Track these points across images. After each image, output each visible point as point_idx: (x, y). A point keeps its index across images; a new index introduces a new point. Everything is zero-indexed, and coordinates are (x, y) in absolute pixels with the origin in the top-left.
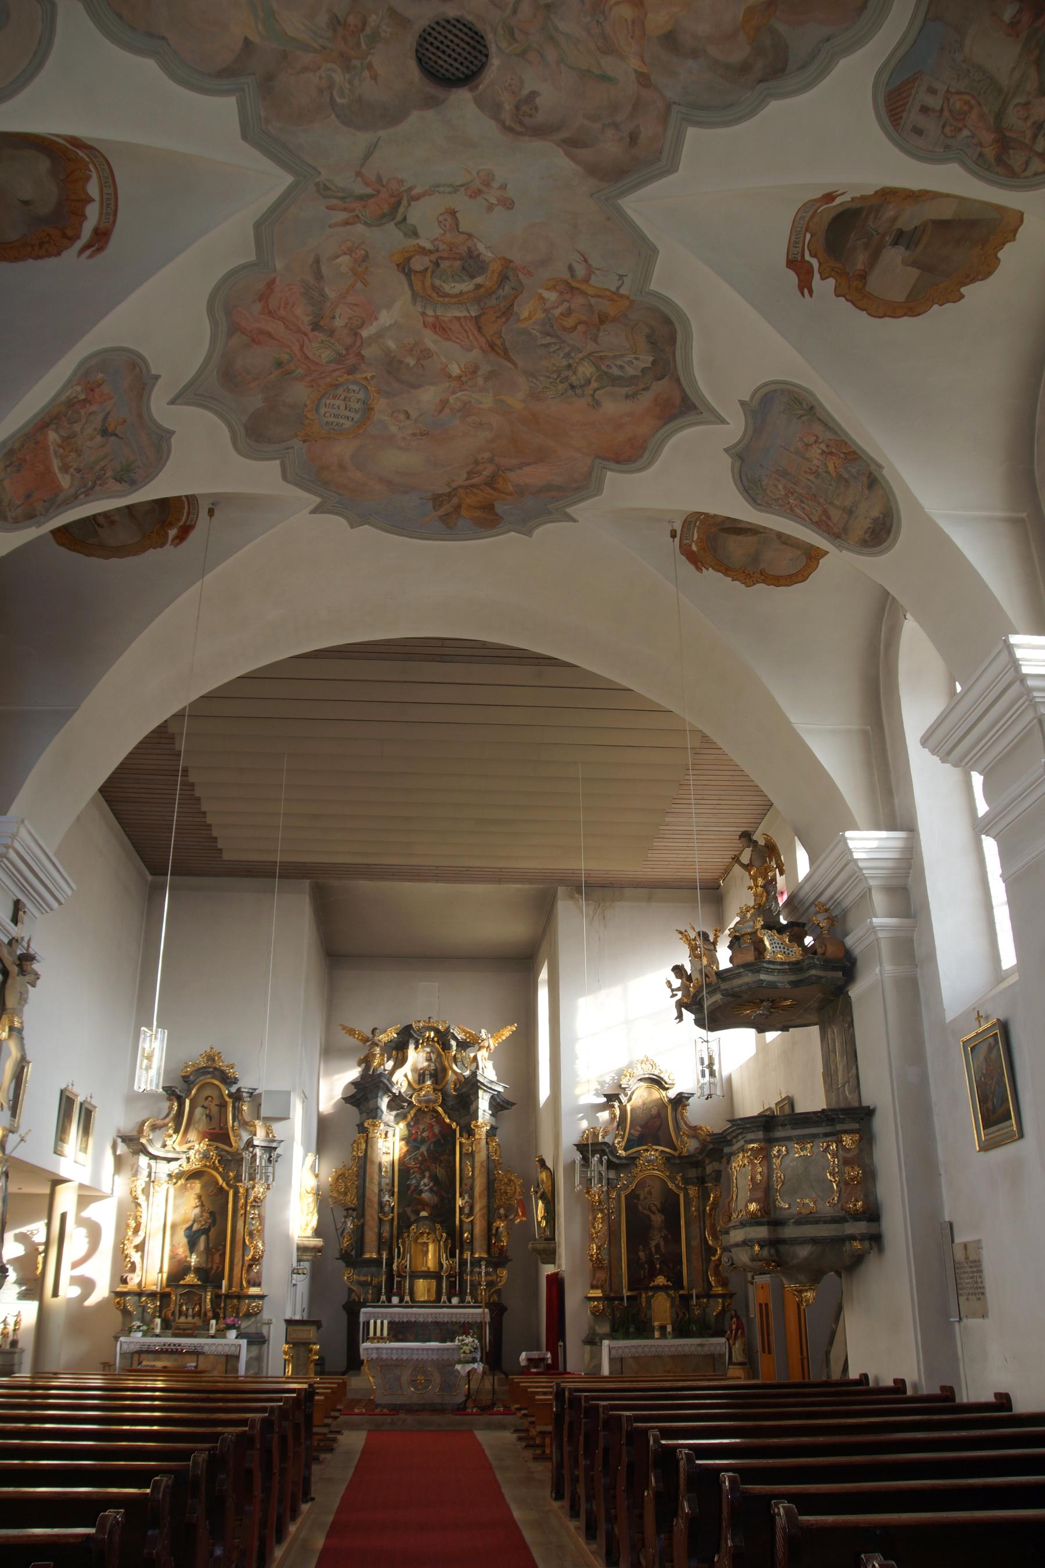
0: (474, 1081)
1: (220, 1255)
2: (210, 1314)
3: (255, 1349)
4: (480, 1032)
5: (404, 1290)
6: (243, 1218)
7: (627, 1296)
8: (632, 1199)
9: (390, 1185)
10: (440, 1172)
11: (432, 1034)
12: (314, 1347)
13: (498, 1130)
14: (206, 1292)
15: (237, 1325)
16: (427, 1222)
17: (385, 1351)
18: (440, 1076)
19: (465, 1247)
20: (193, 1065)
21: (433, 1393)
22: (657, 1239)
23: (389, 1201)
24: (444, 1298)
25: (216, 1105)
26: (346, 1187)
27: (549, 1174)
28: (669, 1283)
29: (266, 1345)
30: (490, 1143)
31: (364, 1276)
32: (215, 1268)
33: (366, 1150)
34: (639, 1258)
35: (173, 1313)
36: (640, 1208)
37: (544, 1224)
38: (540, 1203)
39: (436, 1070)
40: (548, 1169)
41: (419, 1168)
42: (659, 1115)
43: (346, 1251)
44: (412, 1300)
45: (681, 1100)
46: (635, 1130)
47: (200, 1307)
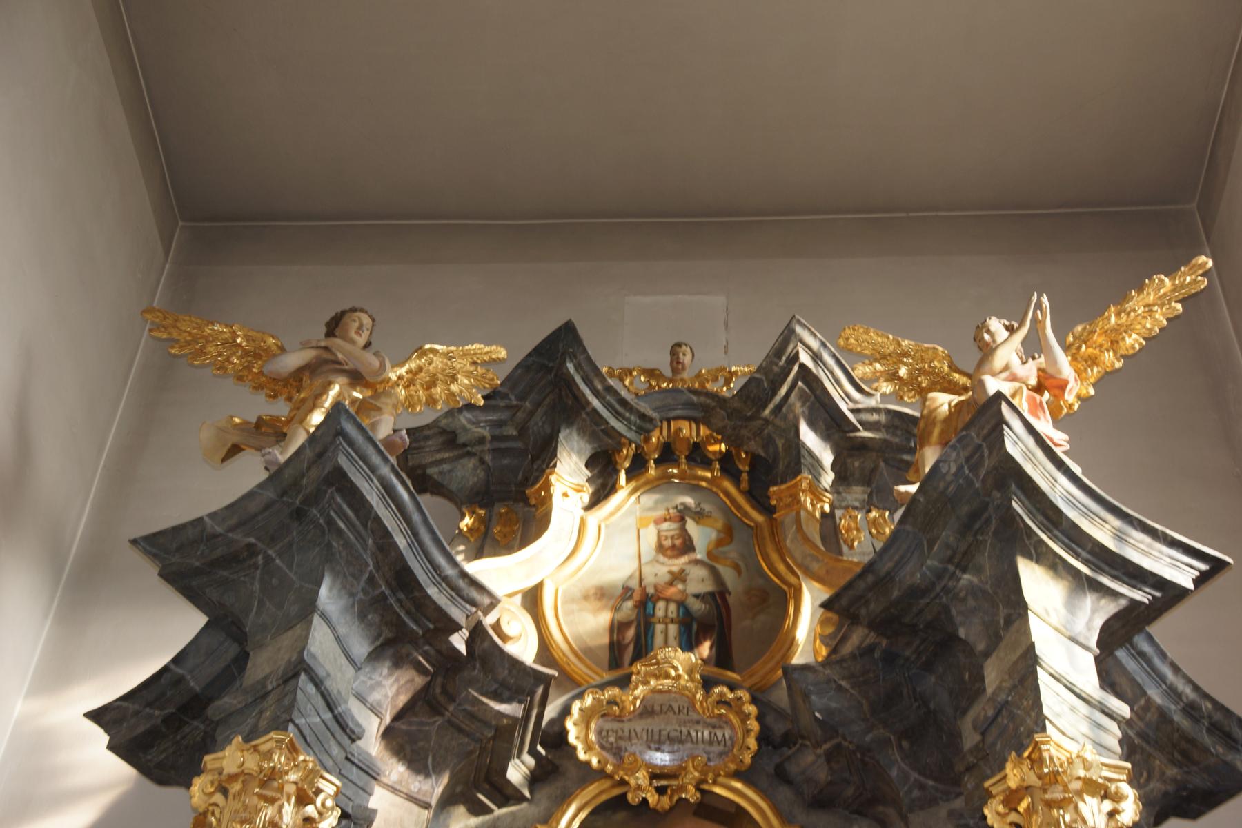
18: (741, 626)
39: (718, 597)
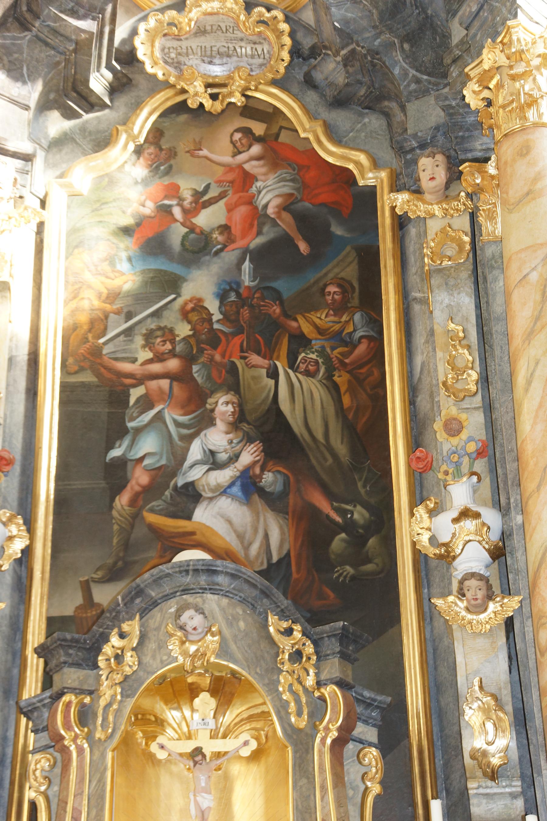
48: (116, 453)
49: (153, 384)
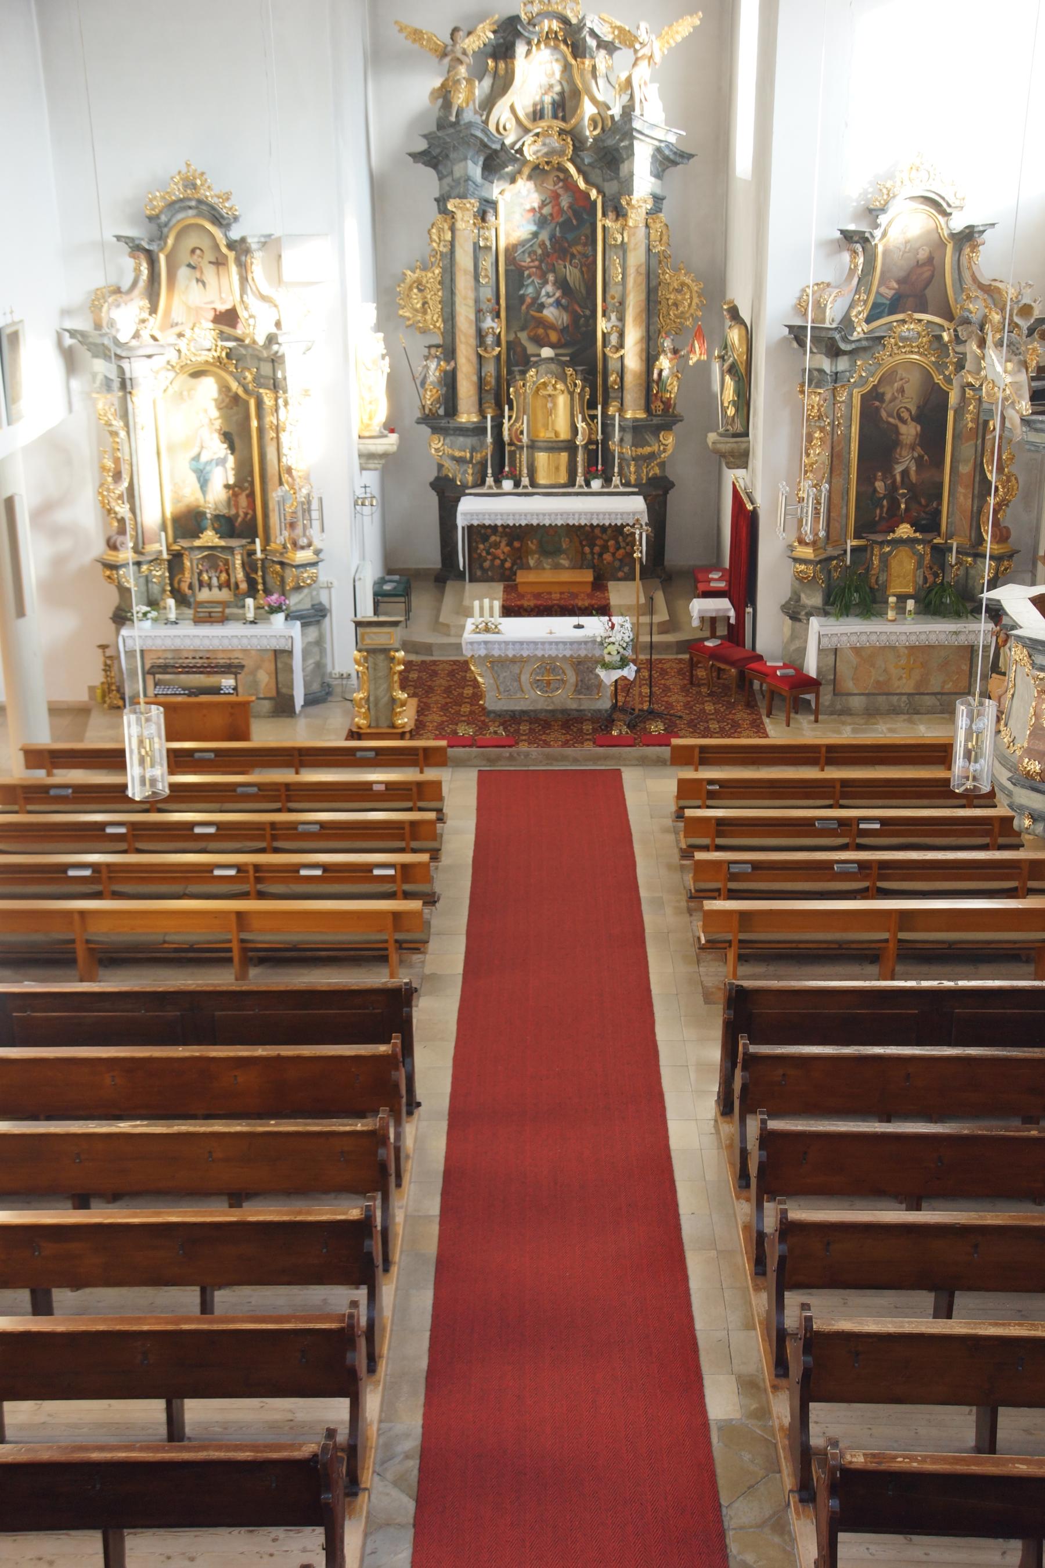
0: (627, 127)
1: (248, 496)
2: (244, 586)
3: (313, 633)
4: (638, 28)
5: (520, 471)
6: (274, 443)
7: (854, 550)
8: (872, 400)
9: (494, 301)
10: (572, 273)
11: (555, 25)
12: (397, 654)
13: (664, 201)
14: (233, 554)
15: (284, 607)
16: (553, 366)
17: (496, 646)
18: (568, 104)
19: (612, 395)
20: (163, 198)
21: (564, 698)
22: (905, 462)
23: (492, 328)
24: (580, 479)
25: (210, 262)
26: (424, 303)
27: (744, 332)
28: (918, 534)
29: (327, 620)
30: (652, 225)
31: (460, 450)
32: (241, 514)
33: (452, 243)
34: (875, 490)
35: (191, 587)
36: (884, 414)
37: (731, 411)
38: (727, 378)
39: (562, 94)
40: (742, 322)
41: (538, 268)
42: (930, 260)
43: (430, 410)
44: (533, 484)
45: (968, 237)
46: (888, 287)
47: (228, 574)
48: (521, 292)
49: (531, 270)
